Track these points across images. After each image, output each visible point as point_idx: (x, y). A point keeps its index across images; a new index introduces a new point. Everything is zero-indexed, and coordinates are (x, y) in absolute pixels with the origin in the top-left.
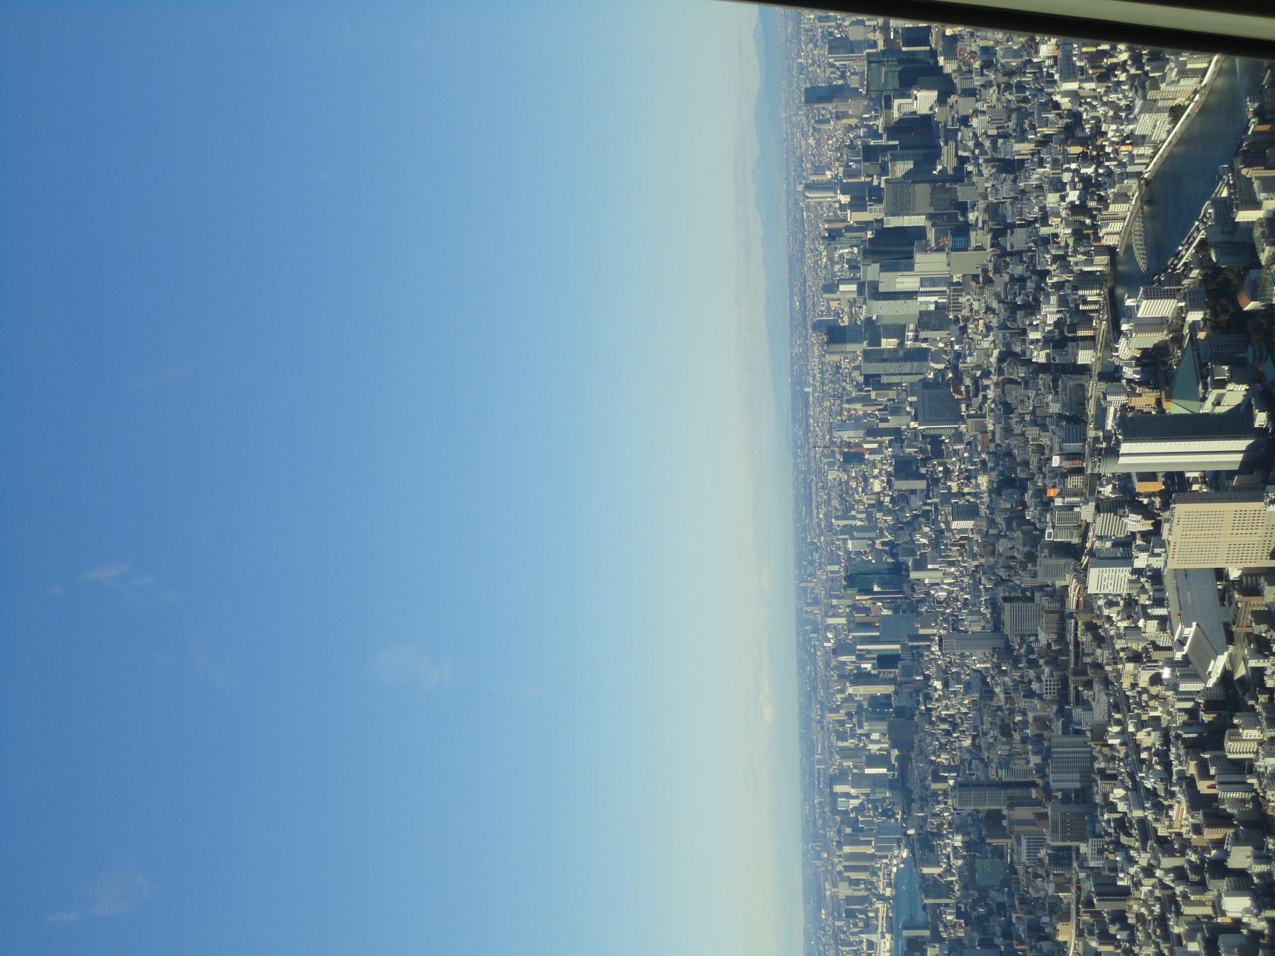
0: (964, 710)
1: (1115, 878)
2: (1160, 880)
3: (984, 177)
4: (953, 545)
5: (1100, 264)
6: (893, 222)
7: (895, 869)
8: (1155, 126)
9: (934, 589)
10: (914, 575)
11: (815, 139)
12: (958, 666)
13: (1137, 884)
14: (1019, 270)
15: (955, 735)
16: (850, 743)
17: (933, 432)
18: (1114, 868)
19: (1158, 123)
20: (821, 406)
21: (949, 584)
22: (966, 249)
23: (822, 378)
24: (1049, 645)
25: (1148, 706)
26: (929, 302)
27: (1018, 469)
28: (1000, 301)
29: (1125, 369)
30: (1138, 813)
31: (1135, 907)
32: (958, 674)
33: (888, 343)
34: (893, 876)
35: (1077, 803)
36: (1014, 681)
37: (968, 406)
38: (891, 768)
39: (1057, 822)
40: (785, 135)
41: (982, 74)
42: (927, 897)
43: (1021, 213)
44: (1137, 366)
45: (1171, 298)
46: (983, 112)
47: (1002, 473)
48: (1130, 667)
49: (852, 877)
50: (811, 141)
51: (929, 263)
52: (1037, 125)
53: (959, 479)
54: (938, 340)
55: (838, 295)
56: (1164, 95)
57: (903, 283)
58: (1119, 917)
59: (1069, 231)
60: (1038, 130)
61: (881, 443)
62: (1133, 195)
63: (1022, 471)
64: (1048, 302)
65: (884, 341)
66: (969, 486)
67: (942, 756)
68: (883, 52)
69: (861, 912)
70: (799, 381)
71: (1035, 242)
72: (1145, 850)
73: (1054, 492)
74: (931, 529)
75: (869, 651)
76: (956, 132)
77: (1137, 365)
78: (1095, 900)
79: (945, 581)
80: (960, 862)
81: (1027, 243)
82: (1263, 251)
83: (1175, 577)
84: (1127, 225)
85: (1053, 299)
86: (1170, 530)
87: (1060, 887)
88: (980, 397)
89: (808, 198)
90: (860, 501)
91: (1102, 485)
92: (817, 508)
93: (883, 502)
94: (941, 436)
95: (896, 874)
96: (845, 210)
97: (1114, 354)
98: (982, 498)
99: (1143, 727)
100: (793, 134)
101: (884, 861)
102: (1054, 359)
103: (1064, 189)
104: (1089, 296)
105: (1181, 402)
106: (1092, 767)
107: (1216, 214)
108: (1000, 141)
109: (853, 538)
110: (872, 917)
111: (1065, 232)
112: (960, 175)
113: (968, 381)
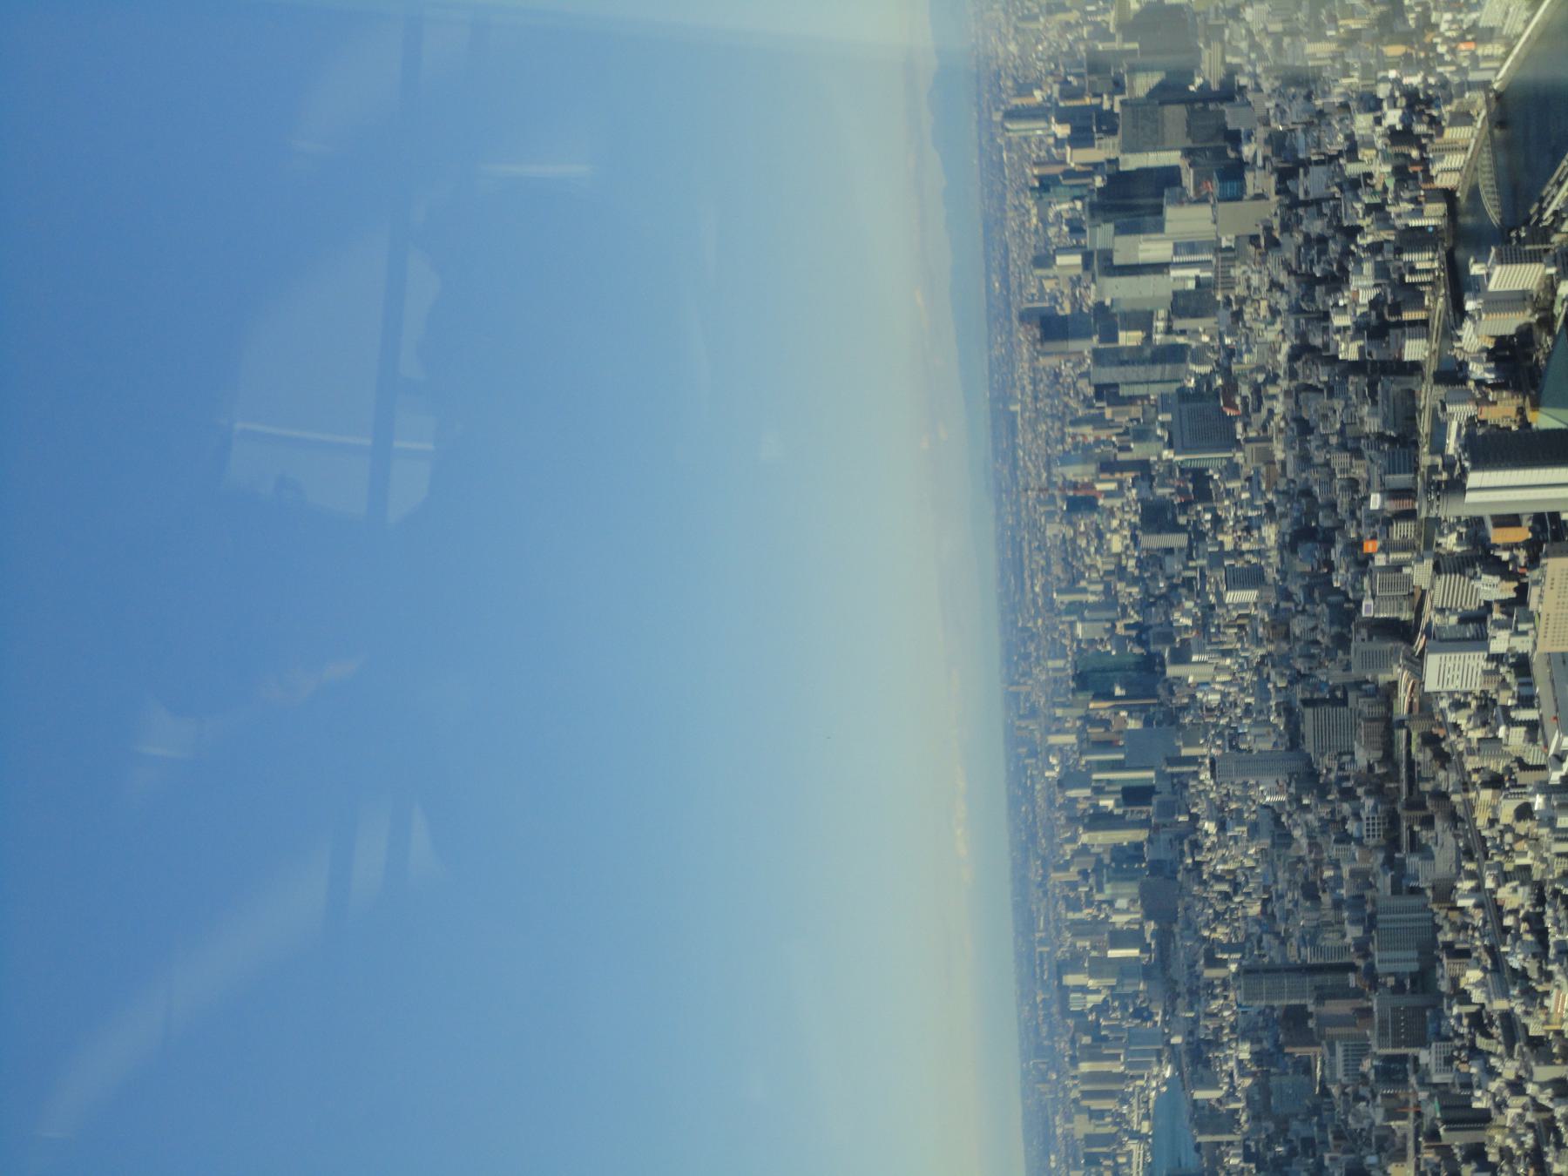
0: (1249, 863)
1: (1469, 1098)
2: (1534, 1099)
4: (1228, 626)
5: (1433, 216)
6: (1132, 162)
7: (1153, 1094)
8: (1506, 14)
9: (1201, 691)
10: (1172, 671)
11: (1017, 43)
12: (1239, 799)
13: (1501, 1106)
14: (1317, 227)
15: (1237, 899)
16: (1086, 914)
17: (1195, 465)
18: (1468, 1085)
19: (1511, 9)
20: (1034, 431)
21: (1224, 683)
22: (1238, 197)
24: (1370, 768)
25: (1512, 850)
26: (1186, 278)
27: (1321, 514)
28: (1291, 272)
29: (1472, 366)
30: (1500, 1005)
31: (1498, 1138)
32: (1239, 812)
33: (1129, 338)
34: (1151, 1104)
35: (1413, 992)
36: (1321, 819)
38: (1145, 948)
39: (1386, 1021)
40: (973, 40)
42: (1201, 1133)
43: (1318, 144)
44: (1488, 360)
45: (1536, 262)
47: (1297, 521)
48: (1486, 795)
49: (1093, 1108)
50: (1013, 48)
52: (1338, 16)
54: (1202, 332)
55: (1055, 271)
57: (1148, 250)
58: (1476, 1153)
59: (1387, 169)
60: (1341, 22)
61: (1121, 483)
62: (1478, 114)
63: (1326, 517)
66: (1246, 540)
67: (1219, 930)
69: (1107, 1156)
70: (1002, 396)
71: (1340, 186)
72: (1511, 1056)
73: (1374, 546)
74: (1196, 604)
75: (1110, 782)
76: (1221, 29)
77: (1488, 360)
78: (1441, 1131)
79: (1218, 679)
80: (1248, 1082)
81: (1328, 187)
83: (1549, 663)
84: (1471, 158)
85: (1368, 268)
86: (1541, 596)
87: (1392, 1114)
88: (1264, 412)
89: (1008, 130)
90: (1092, 567)
91: (1442, 534)
92: (1032, 577)
93: (1125, 568)
94: (1207, 470)
95: (1156, 1102)
97: (1457, 345)
98: (1269, 557)
99: (1506, 881)
101: (1140, 1083)
104: (1419, 261)
105: (1553, 411)
106: (1435, 939)
108: (1287, 41)
109: (1083, 620)
110: (1124, 1164)
111: (1382, 171)
113: (1245, 390)
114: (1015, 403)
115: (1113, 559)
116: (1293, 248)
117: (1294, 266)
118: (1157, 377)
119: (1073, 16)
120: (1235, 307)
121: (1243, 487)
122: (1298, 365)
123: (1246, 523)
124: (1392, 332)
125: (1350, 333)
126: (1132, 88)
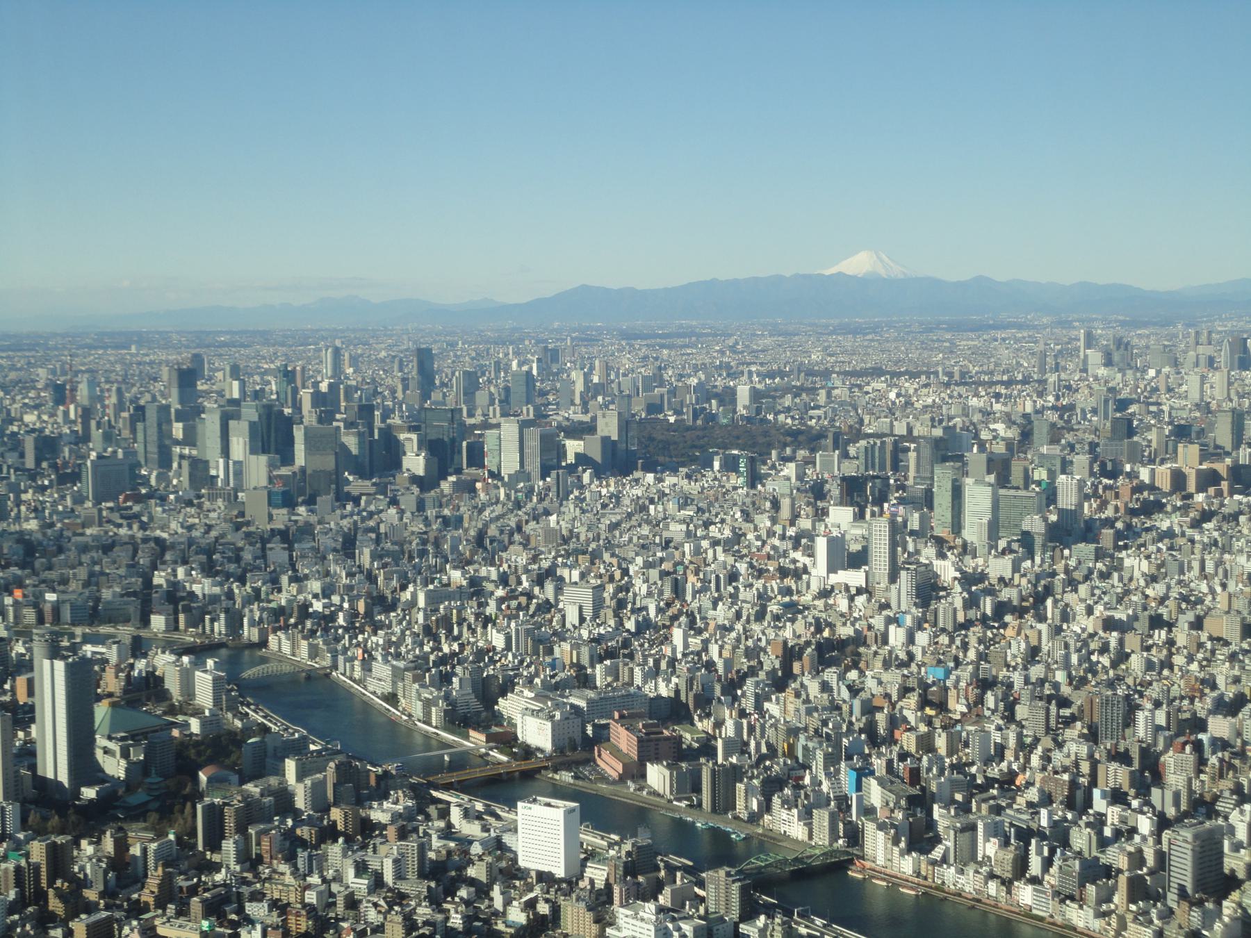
3: (339, 521)
5: (250, 633)
6: (299, 434)
8: (380, 680)
14: (247, 556)
17: (84, 474)
20: (116, 362)
22: (270, 504)
23: (145, 363)
26: (218, 469)
27: (44, 560)
28: (217, 539)
29: (144, 661)
33: (178, 430)
37: (111, 509)
41: (437, 517)
43: (303, 557)
44: (147, 672)
46: (401, 519)
47: (40, 543)
50: (383, 354)
51: (258, 469)
53: (34, 501)
54: (180, 478)
56: (408, 688)
57: (238, 444)
59: (283, 603)
61: (74, 422)
63: (42, 563)
65: (180, 425)
68: (463, 424)
70: (143, 339)
71: (274, 571)
76: (385, 495)
81: (274, 563)
82: (256, 786)
85: (217, 590)
88: (120, 521)
89: (326, 350)
90: (13, 401)
91: (24, 643)
92: (8, 357)
93: (12, 424)
96: (313, 387)
97: (159, 651)
100: (390, 336)
102: (156, 592)
103: (324, 598)
105: (108, 717)
107: (294, 740)
108: (373, 536)
111: (282, 599)
112: (342, 498)
113: (136, 508)
114: (137, 349)
115: (19, 415)
116: (233, 540)
118: (149, 449)
120: (195, 501)
121: (67, 507)
122: (152, 544)
123: (40, 508)
125: (172, 578)
126: (347, 434)
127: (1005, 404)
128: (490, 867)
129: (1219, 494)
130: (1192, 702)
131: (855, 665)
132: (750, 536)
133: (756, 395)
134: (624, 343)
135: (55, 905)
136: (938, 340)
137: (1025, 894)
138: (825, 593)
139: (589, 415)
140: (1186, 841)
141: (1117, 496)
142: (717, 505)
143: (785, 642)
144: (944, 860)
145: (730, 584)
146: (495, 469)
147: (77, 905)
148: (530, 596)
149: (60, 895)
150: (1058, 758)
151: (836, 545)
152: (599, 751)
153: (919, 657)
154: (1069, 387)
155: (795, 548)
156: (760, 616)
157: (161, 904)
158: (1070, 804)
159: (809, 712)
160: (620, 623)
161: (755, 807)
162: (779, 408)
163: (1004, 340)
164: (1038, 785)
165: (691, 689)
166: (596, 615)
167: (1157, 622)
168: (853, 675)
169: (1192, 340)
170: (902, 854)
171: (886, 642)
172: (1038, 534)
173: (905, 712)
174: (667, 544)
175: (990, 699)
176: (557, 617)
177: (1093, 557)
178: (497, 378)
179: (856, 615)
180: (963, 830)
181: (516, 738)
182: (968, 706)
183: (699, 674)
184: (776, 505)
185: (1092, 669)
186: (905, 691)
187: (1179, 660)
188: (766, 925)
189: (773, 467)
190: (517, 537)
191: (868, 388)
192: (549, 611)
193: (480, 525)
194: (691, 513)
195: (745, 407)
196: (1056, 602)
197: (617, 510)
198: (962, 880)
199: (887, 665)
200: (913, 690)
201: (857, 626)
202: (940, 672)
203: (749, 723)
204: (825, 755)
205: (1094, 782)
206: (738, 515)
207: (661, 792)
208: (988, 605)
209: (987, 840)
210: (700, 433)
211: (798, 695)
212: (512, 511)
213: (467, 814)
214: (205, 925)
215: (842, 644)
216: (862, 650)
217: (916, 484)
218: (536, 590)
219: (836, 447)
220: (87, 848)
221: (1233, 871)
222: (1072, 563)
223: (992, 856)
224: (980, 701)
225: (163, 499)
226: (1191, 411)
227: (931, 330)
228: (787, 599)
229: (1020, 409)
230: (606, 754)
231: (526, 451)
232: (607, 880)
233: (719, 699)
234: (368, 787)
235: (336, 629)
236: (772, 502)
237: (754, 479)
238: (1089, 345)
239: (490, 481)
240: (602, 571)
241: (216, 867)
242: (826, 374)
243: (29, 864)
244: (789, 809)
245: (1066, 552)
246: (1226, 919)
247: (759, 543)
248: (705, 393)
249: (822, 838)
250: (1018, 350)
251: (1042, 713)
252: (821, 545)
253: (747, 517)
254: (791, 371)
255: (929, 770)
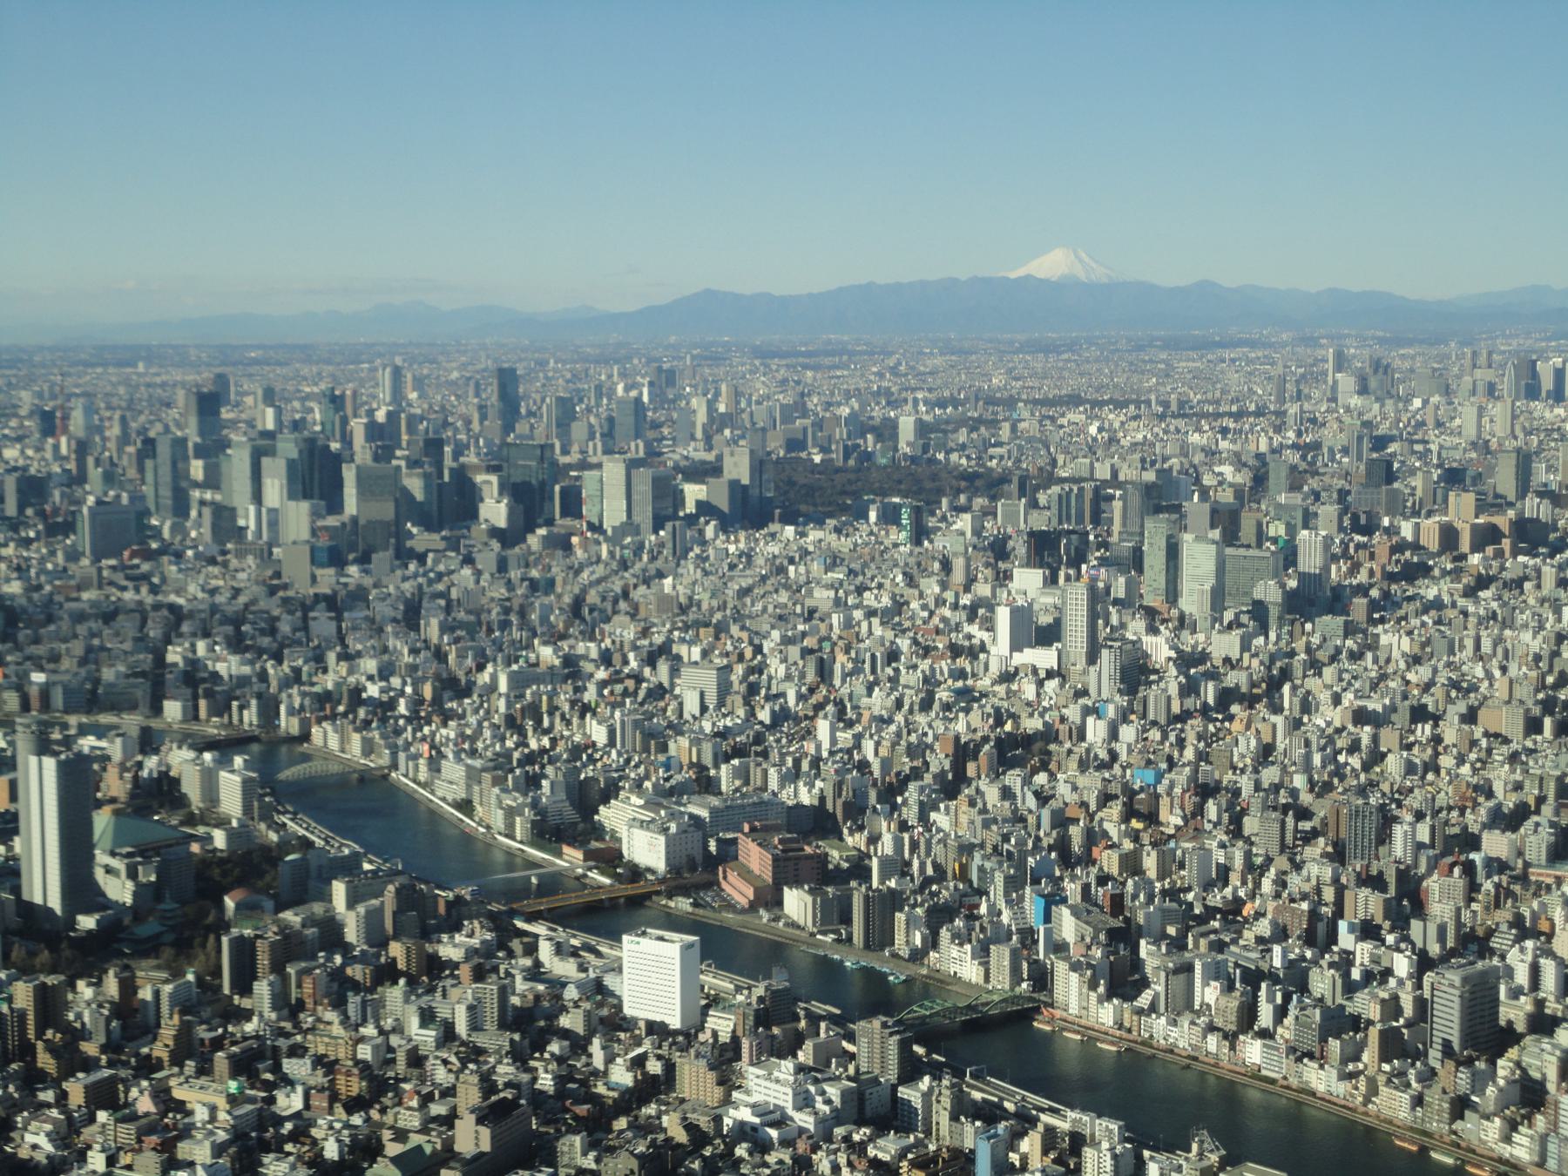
3: (399, 584)
6: (349, 474)
14: (285, 628)
17: (79, 524)
20: (119, 383)
22: (313, 562)
26: (248, 519)
28: (246, 606)
29: (155, 759)
33: (197, 469)
37: (113, 568)
41: (523, 580)
43: (355, 628)
44: (160, 772)
46: (478, 582)
47: (24, 611)
50: (455, 375)
51: (298, 519)
54: (199, 530)
55: (261, 406)
59: (330, 686)
61: (66, 458)
64: (243, 663)
68: (554, 463)
70: (152, 355)
71: (319, 646)
76: (458, 552)
85: (247, 670)
88: (125, 583)
108: (442, 602)
111: (329, 682)
112: (404, 555)
113: (146, 567)
117: (253, 608)
119: (476, 426)
120: (220, 559)
122: (165, 612)
124: (188, 691)
126: (409, 475)
127: (1234, 441)
128: (588, 1014)
129: (1499, 554)
130: (1462, 814)
131: (1044, 766)
132: (915, 605)
133: (922, 429)
134: (757, 362)
135: (45, 1061)
136: (1151, 361)
137: (1253, 1051)
138: (1008, 677)
139: (714, 453)
140: (1452, 986)
141: (1372, 557)
142: (873, 566)
143: (957, 738)
144: (1153, 1008)
145: (889, 665)
146: (595, 521)
147: (73, 1062)
148: (638, 678)
149: (51, 1048)
150: (1295, 882)
151: (1021, 617)
152: (725, 872)
153: (1123, 757)
154: (1314, 421)
155: (971, 620)
156: (926, 705)
157: (177, 1059)
158: (1309, 939)
159: (986, 825)
160: (751, 714)
161: (918, 941)
162: (951, 444)
163: (1233, 361)
164: (1269, 916)
165: (840, 795)
166: (721, 703)
167: (1420, 714)
168: (1041, 779)
169: (1467, 362)
170: (1100, 1001)
171: (1082, 737)
172: (1275, 604)
173: (1106, 825)
174: (810, 614)
175: (1212, 809)
176: (672, 706)
177: (1341, 632)
178: (598, 405)
179: (1045, 704)
180: (1176, 971)
181: (621, 856)
182: (1185, 818)
183: (849, 777)
184: (946, 566)
185: (1339, 772)
186: (1106, 799)
187: (1446, 761)
188: (931, 1089)
189: (944, 518)
190: (623, 605)
191: (1064, 421)
192: (662, 698)
193: (577, 590)
194: (841, 576)
195: (908, 444)
196: (1294, 688)
197: (748, 572)
198: (1174, 1033)
199: (1083, 766)
200: (1116, 797)
201: (1047, 718)
202: (1150, 776)
203: (911, 838)
204: (1006, 878)
205: (1339, 913)
206: (899, 578)
207: (802, 923)
208: (1210, 693)
209: (1206, 984)
210: (852, 476)
211: (972, 803)
212: (616, 573)
213: (560, 950)
214: (233, 1086)
215: (1027, 741)
216: (1052, 747)
217: (1121, 540)
218: (647, 671)
219: (1022, 493)
220: (85, 990)
221: (1510, 1023)
222: (1315, 640)
223: (1212, 1003)
224: (1199, 811)
225: (179, 556)
226: (1465, 450)
227: (1140, 348)
228: (960, 684)
229: (1252, 447)
230: (733, 876)
231: (635, 497)
232: (734, 1031)
233: (874, 808)
234: (436, 916)
235: (396, 719)
236: (941, 563)
237: (920, 533)
238: (1339, 368)
239: (589, 534)
240: (729, 648)
241: (247, 1015)
242: (1011, 403)
243: (11, 1009)
244: (961, 945)
245: (1308, 626)
246: (1501, 1082)
247: (926, 614)
248: (859, 426)
249: (1001, 981)
250: (1250, 374)
251: (1277, 826)
252: (1003, 616)
253: (911, 581)
254: (967, 399)
255: (1135, 897)
